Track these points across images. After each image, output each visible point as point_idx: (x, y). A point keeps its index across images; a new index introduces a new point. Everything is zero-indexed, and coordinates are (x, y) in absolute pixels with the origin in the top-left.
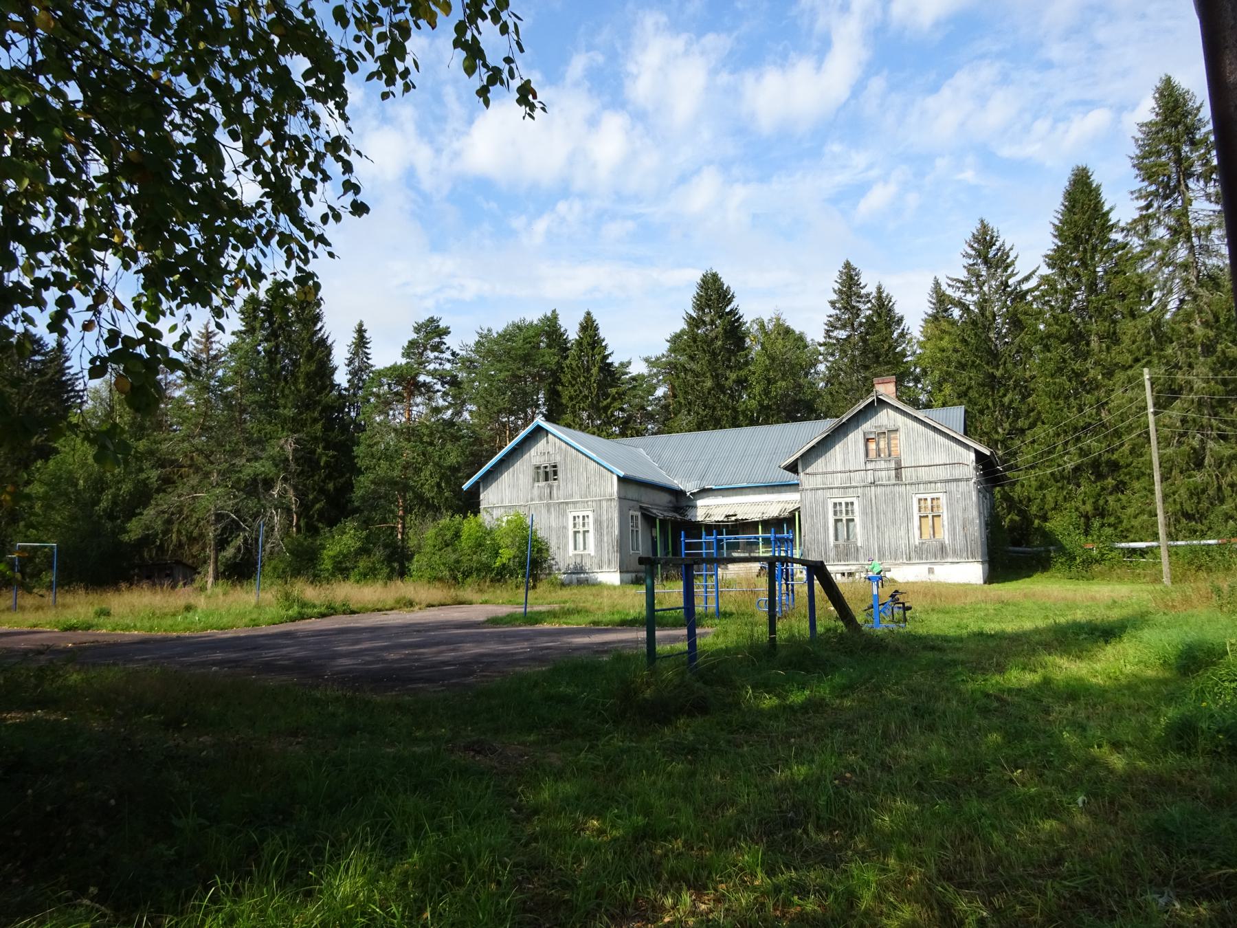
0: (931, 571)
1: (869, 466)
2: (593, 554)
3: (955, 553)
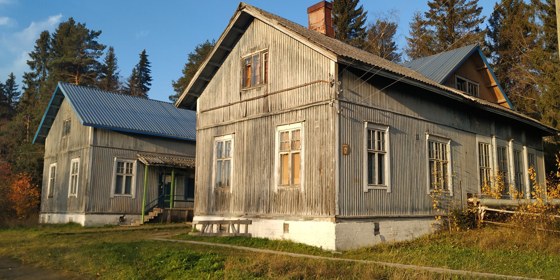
0: (286, 227)
1: (244, 97)
2: (76, 197)
3: (309, 203)
